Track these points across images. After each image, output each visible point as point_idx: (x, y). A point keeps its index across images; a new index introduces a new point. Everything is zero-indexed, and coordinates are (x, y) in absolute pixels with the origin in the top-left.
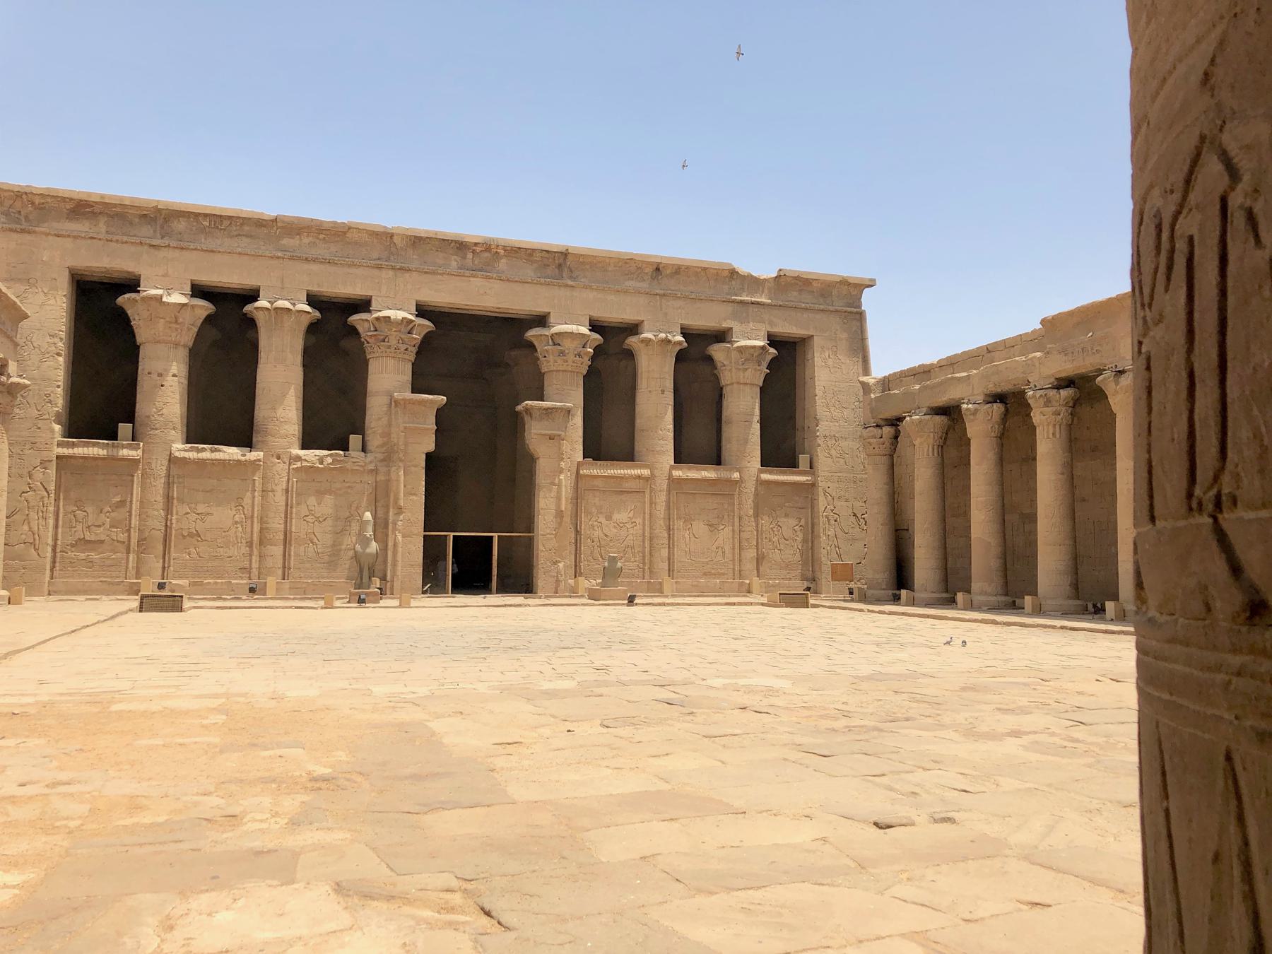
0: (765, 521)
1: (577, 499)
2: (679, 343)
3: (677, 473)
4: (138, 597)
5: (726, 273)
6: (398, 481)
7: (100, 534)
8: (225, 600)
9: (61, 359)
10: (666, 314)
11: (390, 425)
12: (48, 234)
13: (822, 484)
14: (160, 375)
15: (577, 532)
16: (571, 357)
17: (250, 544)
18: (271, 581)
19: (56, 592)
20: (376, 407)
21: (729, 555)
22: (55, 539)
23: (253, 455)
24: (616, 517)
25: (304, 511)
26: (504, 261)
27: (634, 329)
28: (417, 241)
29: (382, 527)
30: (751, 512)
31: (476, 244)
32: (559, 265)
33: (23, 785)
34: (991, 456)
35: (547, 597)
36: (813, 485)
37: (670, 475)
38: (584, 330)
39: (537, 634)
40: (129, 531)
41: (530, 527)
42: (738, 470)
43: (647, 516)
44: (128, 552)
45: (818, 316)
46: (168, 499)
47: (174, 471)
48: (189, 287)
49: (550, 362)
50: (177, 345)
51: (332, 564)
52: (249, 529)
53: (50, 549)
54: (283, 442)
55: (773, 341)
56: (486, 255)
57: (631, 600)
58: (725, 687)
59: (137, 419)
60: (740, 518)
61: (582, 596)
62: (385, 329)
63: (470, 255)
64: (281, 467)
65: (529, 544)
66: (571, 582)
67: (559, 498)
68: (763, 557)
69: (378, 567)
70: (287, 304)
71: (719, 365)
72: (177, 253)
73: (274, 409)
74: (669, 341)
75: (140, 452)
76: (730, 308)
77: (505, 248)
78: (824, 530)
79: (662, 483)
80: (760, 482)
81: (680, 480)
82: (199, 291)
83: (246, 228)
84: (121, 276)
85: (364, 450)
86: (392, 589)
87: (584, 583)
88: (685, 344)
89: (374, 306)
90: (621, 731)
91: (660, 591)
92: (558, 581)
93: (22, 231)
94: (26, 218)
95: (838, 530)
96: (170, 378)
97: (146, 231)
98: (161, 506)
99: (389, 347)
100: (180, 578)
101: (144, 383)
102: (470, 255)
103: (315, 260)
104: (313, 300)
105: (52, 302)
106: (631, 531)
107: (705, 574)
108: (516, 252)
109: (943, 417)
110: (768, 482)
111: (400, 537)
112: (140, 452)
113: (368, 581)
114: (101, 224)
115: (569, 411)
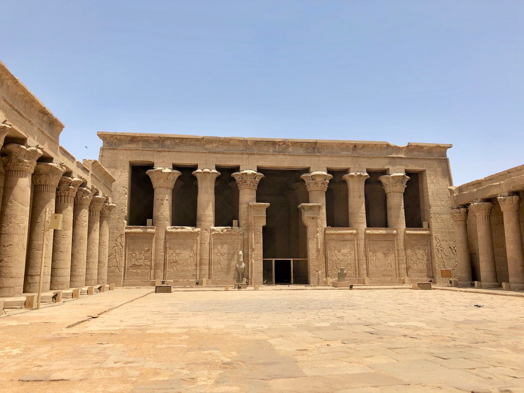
0: (409, 252)
1: (325, 244)
2: (366, 176)
3: (368, 232)
4: (155, 287)
5: (385, 146)
6: (252, 238)
7: (141, 262)
8: (187, 288)
9: (127, 196)
10: (360, 164)
11: (248, 216)
12: (122, 150)
13: (434, 235)
14: (162, 200)
15: (326, 258)
16: (320, 185)
17: (196, 265)
18: (204, 280)
19: (126, 285)
20: (243, 209)
22: (125, 264)
23: (197, 230)
24: (342, 251)
25: (216, 251)
26: (291, 148)
27: (346, 171)
28: (257, 143)
29: (246, 257)
30: (403, 248)
31: (280, 142)
32: (313, 148)
33: (115, 363)
34: (514, 219)
35: (314, 286)
36: (430, 235)
37: (365, 232)
38: (325, 173)
39: (312, 302)
40: (151, 261)
41: (306, 255)
42: (396, 230)
43: (356, 251)
44: (151, 269)
45: (427, 161)
46: (165, 248)
47: (167, 237)
48: (171, 167)
49: (311, 187)
50: (168, 188)
51: (227, 272)
52: (195, 259)
53: (123, 268)
54: (208, 224)
55: (408, 173)
57: (351, 287)
58: (396, 326)
59: (154, 217)
60: (398, 250)
61: (330, 286)
62: (245, 178)
63: (277, 147)
64: (207, 234)
65: (306, 263)
66: (325, 279)
67: (317, 244)
68: (410, 268)
69: (245, 274)
70: (208, 170)
71: (384, 184)
72: (167, 153)
73: (204, 211)
74: (362, 176)
75: (155, 230)
76: (387, 161)
77: (291, 143)
78: (437, 255)
79: (362, 236)
80: (406, 235)
81: (369, 234)
82: (175, 167)
83: (192, 142)
84: (149, 163)
85: (239, 226)
86: (251, 283)
87: (330, 280)
89: (241, 169)
90: (350, 345)
91: (364, 283)
92: (319, 279)
93: (113, 149)
94: (115, 144)
95: (443, 254)
96: (165, 201)
97: (156, 145)
98: (163, 251)
99: (247, 185)
100: (170, 279)
101: (156, 203)
102: (277, 147)
103: (218, 153)
104: (218, 168)
105: (123, 174)
106: (349, 257)
107: (383, 275)
108: (295, 144)
109: (489, 203)
110: (409, 234)
111: (253, 261)
112: (155, 230)
113: (242, 279)
114: (140, 145)
115: (320, 207)
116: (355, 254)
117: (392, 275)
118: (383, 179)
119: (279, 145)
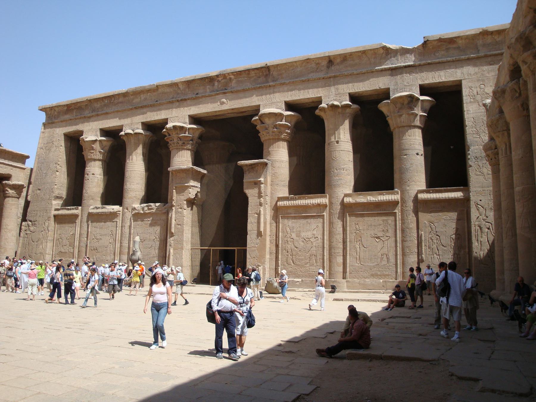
5: (382, 51)
12: (59, 122)
13: (472, 198)
16: (271, 129)
21: (392, 260)
24: (303, 234)
28: (189, 83)
56: (223, 81)
64: (129, 215)
74: (337, 106)
88: (355, 106)
94: (55, 118)
102: (216, 84)
107: (373, 275)
108: (239, 74)
111: (172, 251)
114: (74, 113)
116: (323, 239)
117: (388, 275)
118: (383, 107)
119: (218, 81)
